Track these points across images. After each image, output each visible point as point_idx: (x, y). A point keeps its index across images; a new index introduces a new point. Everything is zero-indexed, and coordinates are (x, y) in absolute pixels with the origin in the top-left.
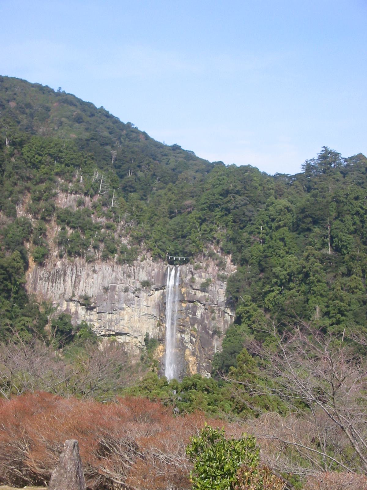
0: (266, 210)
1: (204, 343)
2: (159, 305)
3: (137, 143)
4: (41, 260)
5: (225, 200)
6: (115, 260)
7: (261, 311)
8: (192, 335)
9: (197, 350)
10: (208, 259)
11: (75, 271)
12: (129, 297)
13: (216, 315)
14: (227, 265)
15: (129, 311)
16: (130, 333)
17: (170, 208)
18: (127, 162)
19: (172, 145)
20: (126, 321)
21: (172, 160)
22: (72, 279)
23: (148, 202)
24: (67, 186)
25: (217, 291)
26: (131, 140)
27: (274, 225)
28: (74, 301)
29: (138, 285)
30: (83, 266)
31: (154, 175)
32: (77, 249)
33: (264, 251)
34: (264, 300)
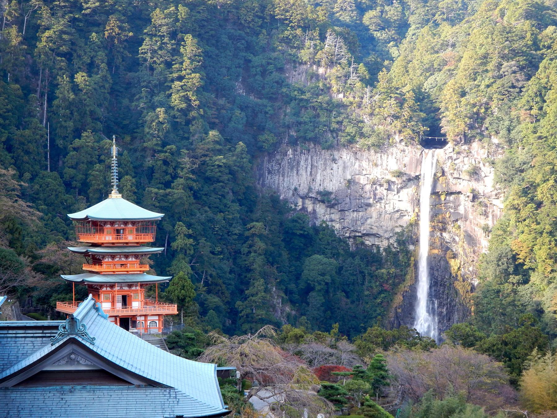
11: (310, 161)
16: (379, 233)
20: (373, 220)
22: (306, 171)
28: (311, 197)
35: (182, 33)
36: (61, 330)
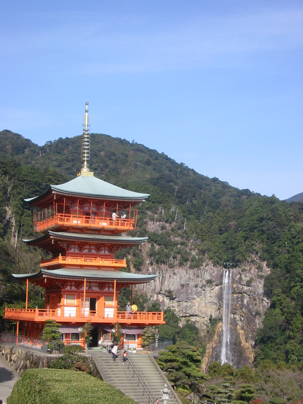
0: (289, 231)
1: (250, 321)
2: (218, 296)
3: (188, 178)
4: (139, 266)
5: (261, 224)
6: (188, 266)
7: (288, 300)
8: (241, 316)
9: (245, 326)
10: (250, 264)
11: (161, 274)
12: (198, 291)
13: (257, 302)
14: (264, 268)
15: (198, 300)
17: (220, 227)
18: (186, 193)
19: (212, 177)
20: (196, 307)
21: (213, 188)
23: (201, 221)
24: (153, 217)
25: (258, 286)
26: (184, 175)
27: (295, 241)
29: (204, 283)
30: (167, 270)
31: (204, 202)
32: (162, 259)
33: (289, 258)
34: (290, 292)
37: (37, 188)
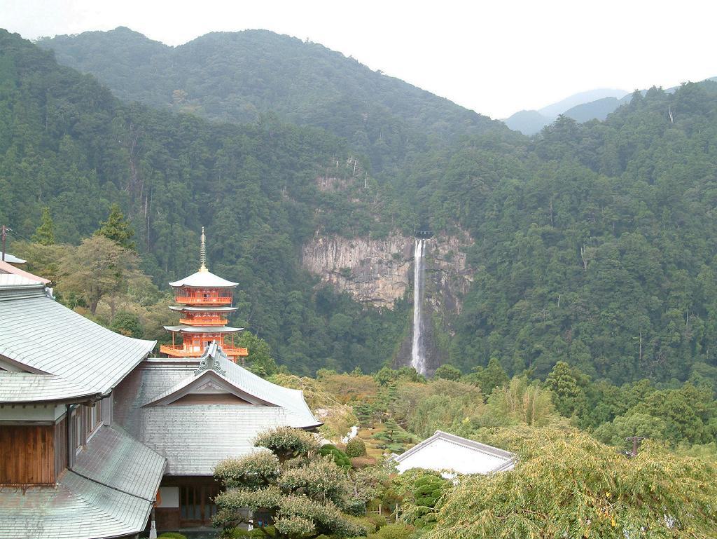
8: (438, 299)
29: (390, 258)
35: (244, 154)
36: (202, 365)
37: (170, 140)
